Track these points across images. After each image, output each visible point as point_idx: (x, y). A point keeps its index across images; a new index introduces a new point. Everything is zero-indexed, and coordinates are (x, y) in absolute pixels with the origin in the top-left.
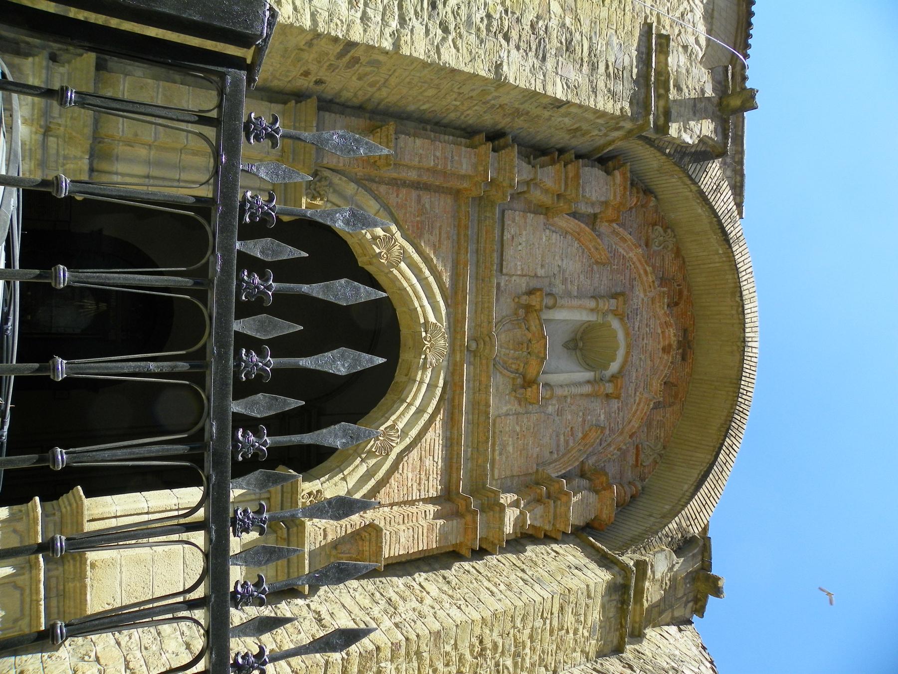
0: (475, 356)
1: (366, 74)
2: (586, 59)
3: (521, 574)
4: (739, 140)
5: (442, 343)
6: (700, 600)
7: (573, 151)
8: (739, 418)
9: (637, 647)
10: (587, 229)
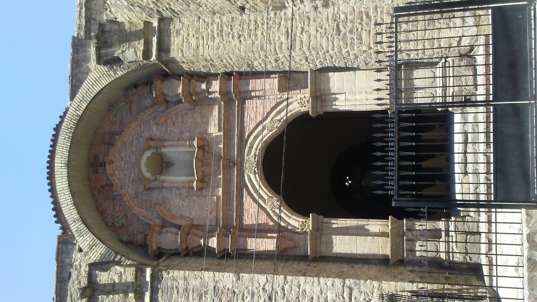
0: (230, 160)
2: (191, 292)
5: (247, 165)
7: (182, 255)
8: (71, 125)
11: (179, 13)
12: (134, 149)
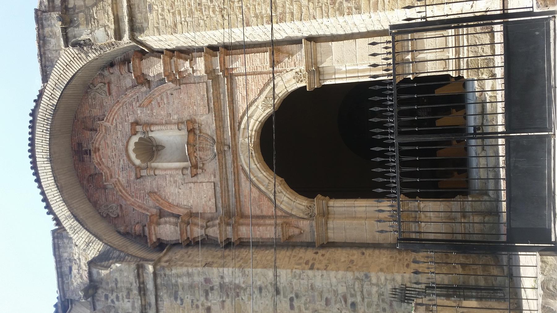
6: (64, 9)
10: (166, 210)
12: (119, 135)
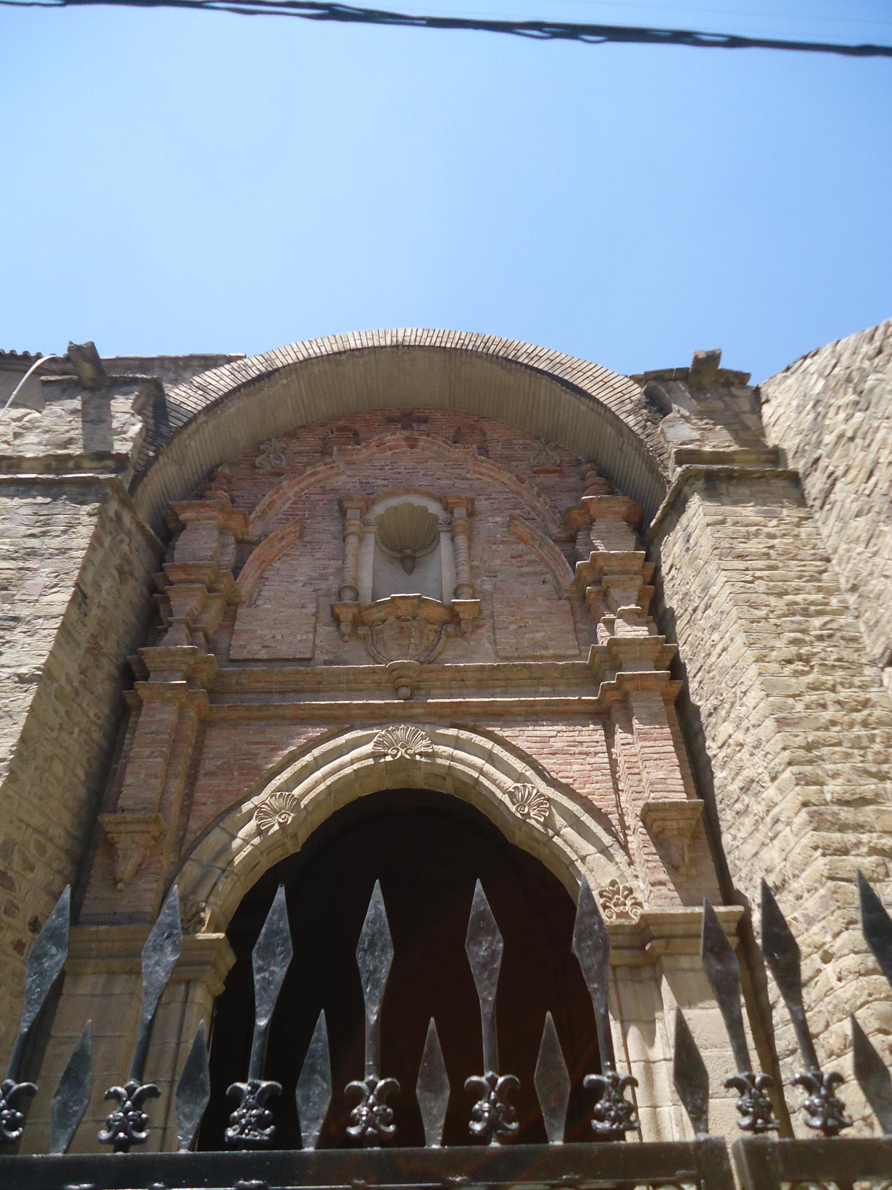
0: (419, 688)
1: (25, 861)
2: (21, 564)
3: (699, 612)
4: (144, 364)
5: (402, 732)
6: (727, 379)
7: (153, 575)
8: (493, 347)
9: (790, 455)
10: (256, 551)
11: (827, 507)
